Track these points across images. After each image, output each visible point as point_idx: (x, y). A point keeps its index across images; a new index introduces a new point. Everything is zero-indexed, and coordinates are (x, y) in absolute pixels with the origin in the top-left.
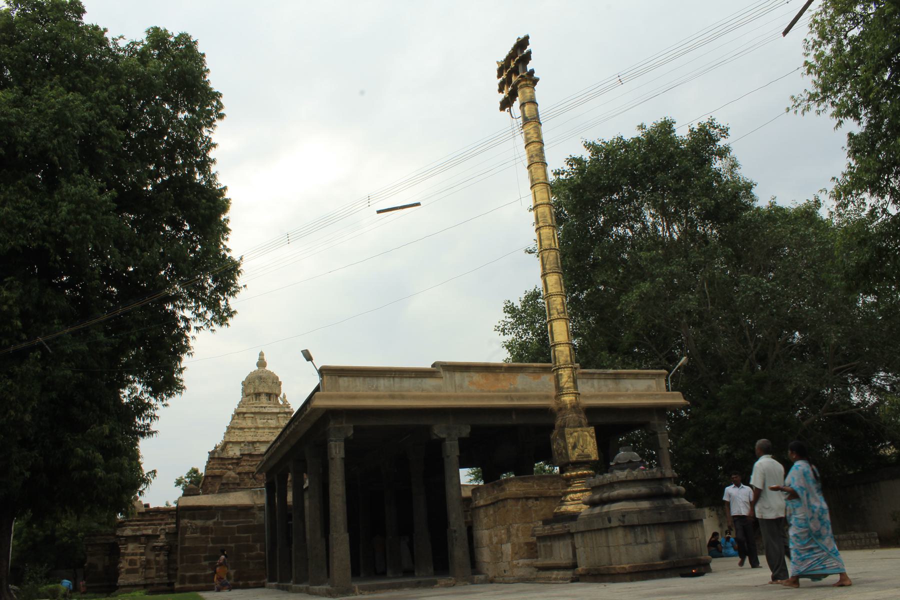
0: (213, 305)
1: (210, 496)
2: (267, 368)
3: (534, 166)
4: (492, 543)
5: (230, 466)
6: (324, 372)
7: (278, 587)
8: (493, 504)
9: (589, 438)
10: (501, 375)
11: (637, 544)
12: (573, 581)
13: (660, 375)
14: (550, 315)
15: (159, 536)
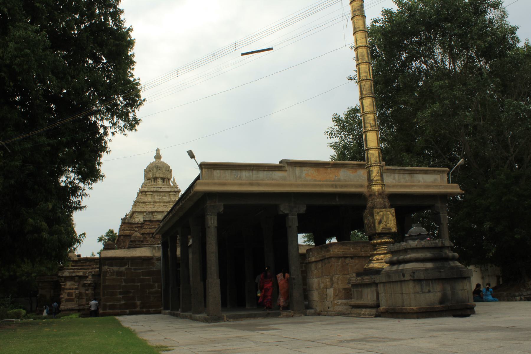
0: (124, 116)
1: (123, 250)
2: (162, 160)
3: (357, 18)
4: (320, 288)
5: (137, 229)
6: (202, 166)
7: (170, 314)
8: (321, 260)
9: (390, 216)
10: (329, 169)
11: (423, 293)
12: (376, 316)
13: (443, 172)
14: (365, 127)
15: (87, 277)
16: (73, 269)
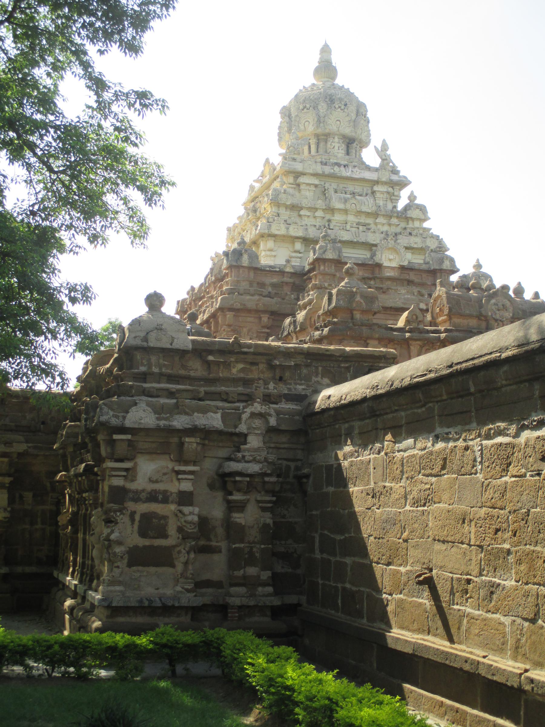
2: (339, 81)
15: (243, 437)
16: (171, 394)
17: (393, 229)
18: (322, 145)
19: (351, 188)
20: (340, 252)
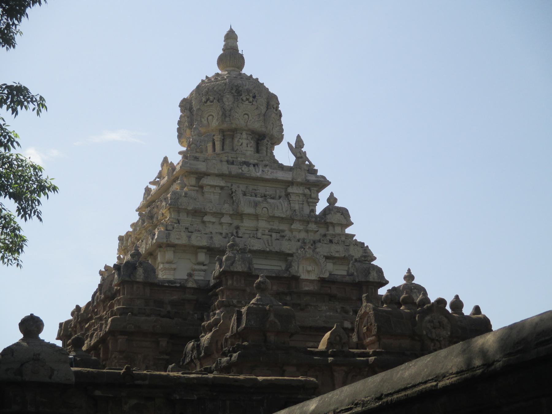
2: (247, 71)
17: (312, 237)
18: (228, 142)
19: (262, 189)
20: (250, 263)
